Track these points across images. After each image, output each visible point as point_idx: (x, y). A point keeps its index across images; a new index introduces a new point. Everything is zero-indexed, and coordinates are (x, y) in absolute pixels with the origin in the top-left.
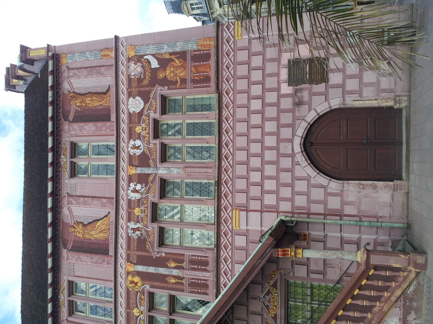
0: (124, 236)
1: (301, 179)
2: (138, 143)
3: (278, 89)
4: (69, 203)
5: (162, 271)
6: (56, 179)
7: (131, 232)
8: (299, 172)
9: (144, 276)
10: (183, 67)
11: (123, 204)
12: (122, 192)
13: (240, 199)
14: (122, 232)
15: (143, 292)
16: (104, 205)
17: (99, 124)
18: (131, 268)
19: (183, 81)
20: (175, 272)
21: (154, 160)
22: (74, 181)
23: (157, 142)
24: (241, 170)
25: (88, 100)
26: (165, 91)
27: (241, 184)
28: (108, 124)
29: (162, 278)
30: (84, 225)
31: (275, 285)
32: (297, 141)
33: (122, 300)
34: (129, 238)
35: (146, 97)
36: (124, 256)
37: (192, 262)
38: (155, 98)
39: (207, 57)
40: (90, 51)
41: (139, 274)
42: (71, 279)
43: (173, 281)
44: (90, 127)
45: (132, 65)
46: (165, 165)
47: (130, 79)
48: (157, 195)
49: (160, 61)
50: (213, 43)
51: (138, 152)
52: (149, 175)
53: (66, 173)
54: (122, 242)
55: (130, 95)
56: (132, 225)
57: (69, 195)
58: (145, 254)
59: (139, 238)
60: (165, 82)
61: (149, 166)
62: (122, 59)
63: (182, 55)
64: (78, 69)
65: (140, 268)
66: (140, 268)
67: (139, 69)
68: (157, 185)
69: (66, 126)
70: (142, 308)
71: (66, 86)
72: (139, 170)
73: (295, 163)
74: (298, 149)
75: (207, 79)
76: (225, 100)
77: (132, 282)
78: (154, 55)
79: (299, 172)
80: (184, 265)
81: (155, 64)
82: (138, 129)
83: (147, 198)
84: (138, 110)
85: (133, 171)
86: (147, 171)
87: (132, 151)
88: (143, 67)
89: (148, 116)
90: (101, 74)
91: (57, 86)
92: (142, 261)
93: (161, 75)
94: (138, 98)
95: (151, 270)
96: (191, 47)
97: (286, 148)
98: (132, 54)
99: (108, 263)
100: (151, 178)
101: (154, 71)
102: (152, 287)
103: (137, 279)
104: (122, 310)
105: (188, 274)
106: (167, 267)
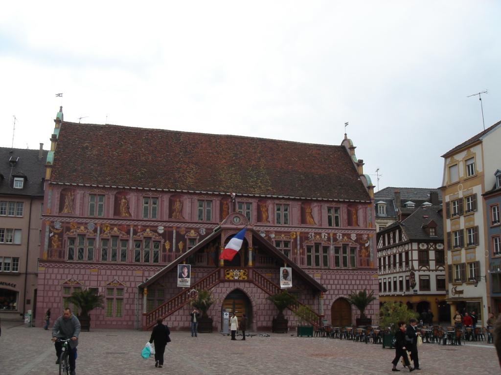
0: (309, 231)
1: (331, 297)
2: (341, 237)
3: (358, 289)
4: (319, 206)
5: (298, 247)
6: (328, 201)
7: (311, 233)
8: (334, 296)
9: (296, 239)
10: (365, 256)
11: (320, 231)
12: (324, 230)
13: (325, 277)
14: (310, 230)
15: (290, 239)
16: (319, 222)
17: (347, 221)
18: (298, 234)
19: (360, 256)
20: (298, 252)
21: (335, 244)
22: (326, 208)
23: (341, 245)
24: (333, 277)
25: (355, 216)
26: (358, 249)
27: (329, 277)
28: (347, 225)
29: (296, 247)
30: (311, 213)
31: (298, 288)
32: (343, 296)
33: (286, 230)
34: (308, 233)
35: (356, 241)
36: (302, 231)
37: (303, 259)
38: (356, 245)
39: (368, 265)
40: (371, 218)
41: (297, 237)
42: (290, 206)
43: (296, 251)
44: (346, 217)
45: (366, 236)
46: (334, 249)
47: (362, 235)
48: (324, 245)
49: (367, 247)
50: (372, 267)
51: (338, 237)
52: (330, 241)
53: (329, 205)
54: (307, 230)
55: (357, 235)
56: (313, 234)
57: (321, 206)
58: (304, 240)
59: (309, 237)
60: (361, 248)
61: (333, 242)
62: (368, 232)
63: (369, 256)
64: (366, 212)
65: (298, 238)
66: (298, 238)
67: (365, 239)
68: (326, 245)
69: (346, 206)
70: (284, 238)
71: (360, 206)
72: (332, 238)
73: (336, 295)
74: (341, 296)
75: (361, 265)
76: (355, 272)
77: (293, 234)
78: (369, 245)
79: (334, 296)
80: (301, 256)
81: (367, 245)
82: (345, 238)
83: (323, 241)
84: (352, 238)
85: (331, 235)
86: (332, 241)
87: (338, 235)
88: (366, 240)
89: (350, 242)
90: (364, 221)
91: (360, 203)
92: (301, 238)
93: (363, 247)
94: (356, 238)
95: (298, 242)
96: (371, 259)
97: (341, 292)
98: (370, 236)
99: (299, 223)
100: (329, 242)
101: (364, 245)
102: (293, 242)
103: (295, 236)
104: (283, 229)
105: (298, 257)
106: (300, 249)
